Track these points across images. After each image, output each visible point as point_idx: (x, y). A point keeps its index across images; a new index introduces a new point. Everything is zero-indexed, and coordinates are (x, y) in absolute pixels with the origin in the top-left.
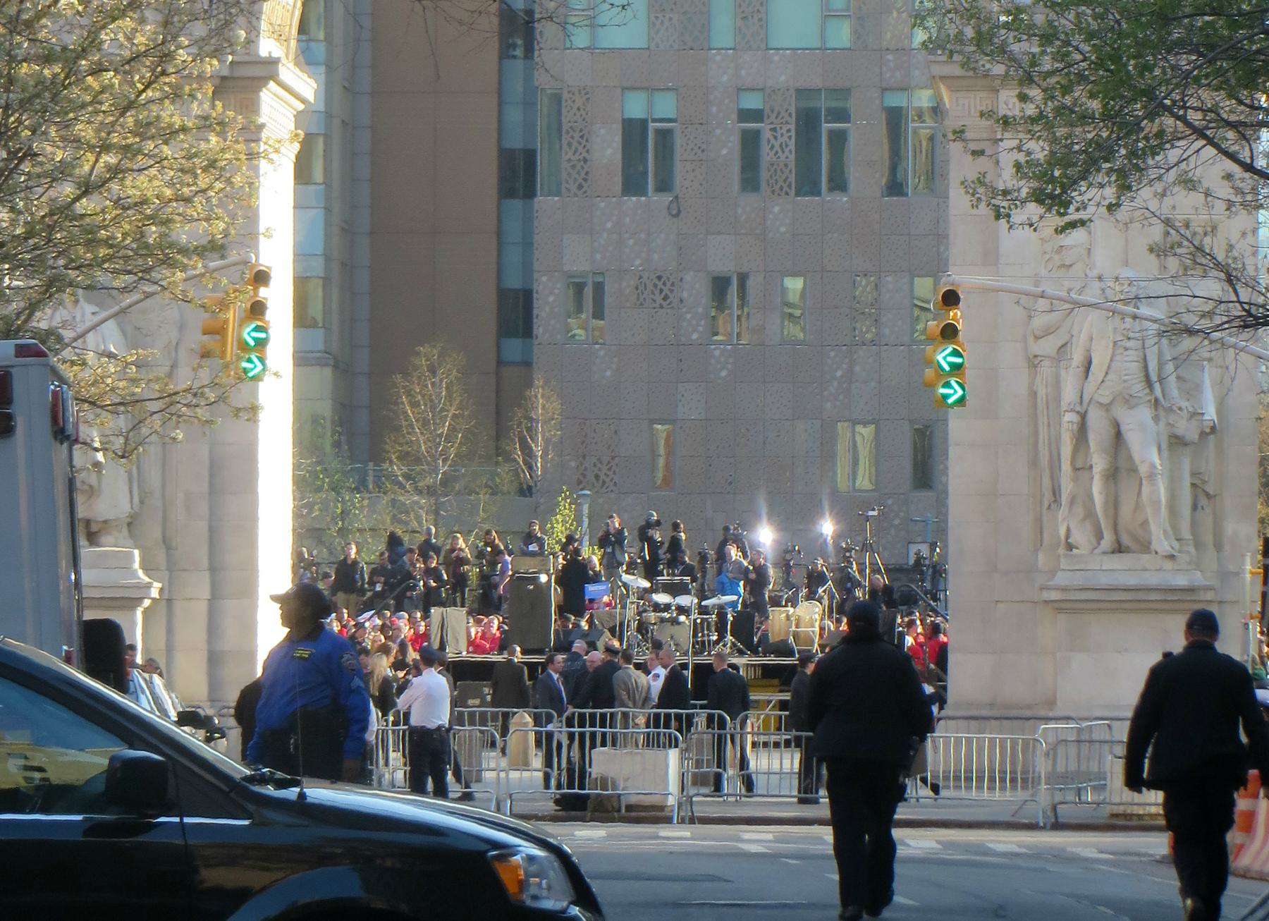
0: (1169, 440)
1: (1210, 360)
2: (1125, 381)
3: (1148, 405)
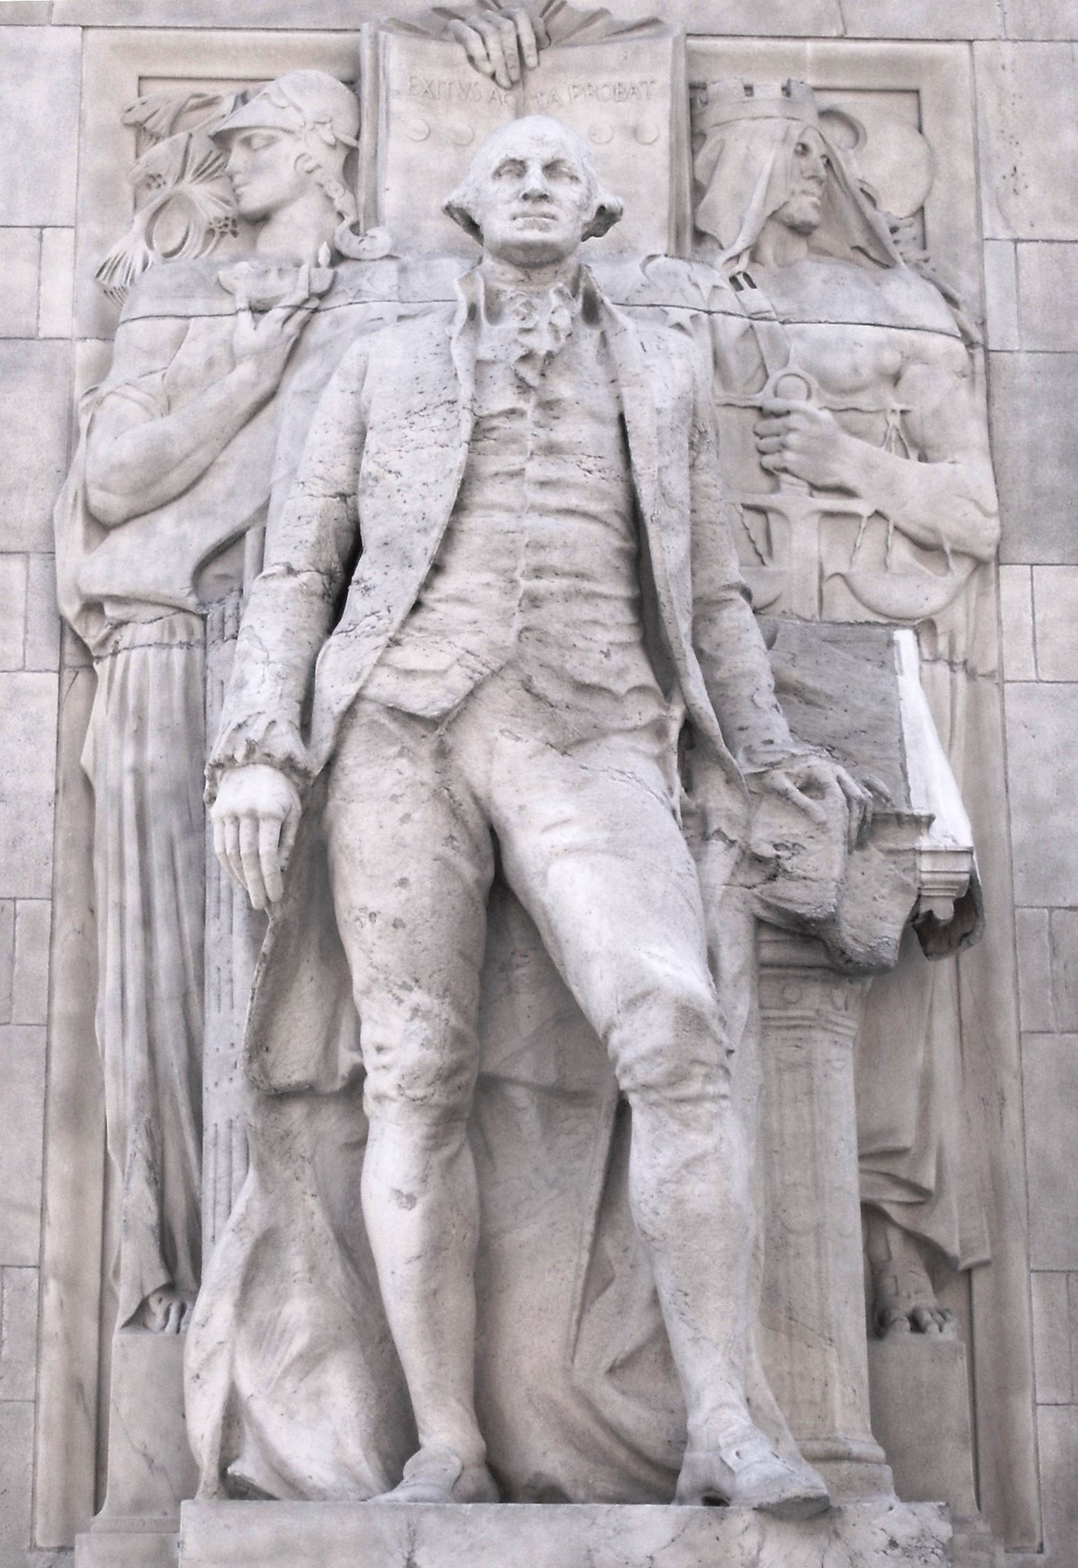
0: (757, 945)
1: (926, 627)
2: (534, 601)
3: (648, 745)
